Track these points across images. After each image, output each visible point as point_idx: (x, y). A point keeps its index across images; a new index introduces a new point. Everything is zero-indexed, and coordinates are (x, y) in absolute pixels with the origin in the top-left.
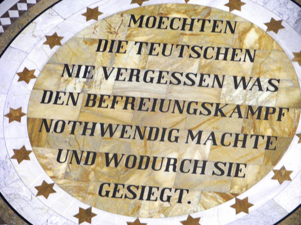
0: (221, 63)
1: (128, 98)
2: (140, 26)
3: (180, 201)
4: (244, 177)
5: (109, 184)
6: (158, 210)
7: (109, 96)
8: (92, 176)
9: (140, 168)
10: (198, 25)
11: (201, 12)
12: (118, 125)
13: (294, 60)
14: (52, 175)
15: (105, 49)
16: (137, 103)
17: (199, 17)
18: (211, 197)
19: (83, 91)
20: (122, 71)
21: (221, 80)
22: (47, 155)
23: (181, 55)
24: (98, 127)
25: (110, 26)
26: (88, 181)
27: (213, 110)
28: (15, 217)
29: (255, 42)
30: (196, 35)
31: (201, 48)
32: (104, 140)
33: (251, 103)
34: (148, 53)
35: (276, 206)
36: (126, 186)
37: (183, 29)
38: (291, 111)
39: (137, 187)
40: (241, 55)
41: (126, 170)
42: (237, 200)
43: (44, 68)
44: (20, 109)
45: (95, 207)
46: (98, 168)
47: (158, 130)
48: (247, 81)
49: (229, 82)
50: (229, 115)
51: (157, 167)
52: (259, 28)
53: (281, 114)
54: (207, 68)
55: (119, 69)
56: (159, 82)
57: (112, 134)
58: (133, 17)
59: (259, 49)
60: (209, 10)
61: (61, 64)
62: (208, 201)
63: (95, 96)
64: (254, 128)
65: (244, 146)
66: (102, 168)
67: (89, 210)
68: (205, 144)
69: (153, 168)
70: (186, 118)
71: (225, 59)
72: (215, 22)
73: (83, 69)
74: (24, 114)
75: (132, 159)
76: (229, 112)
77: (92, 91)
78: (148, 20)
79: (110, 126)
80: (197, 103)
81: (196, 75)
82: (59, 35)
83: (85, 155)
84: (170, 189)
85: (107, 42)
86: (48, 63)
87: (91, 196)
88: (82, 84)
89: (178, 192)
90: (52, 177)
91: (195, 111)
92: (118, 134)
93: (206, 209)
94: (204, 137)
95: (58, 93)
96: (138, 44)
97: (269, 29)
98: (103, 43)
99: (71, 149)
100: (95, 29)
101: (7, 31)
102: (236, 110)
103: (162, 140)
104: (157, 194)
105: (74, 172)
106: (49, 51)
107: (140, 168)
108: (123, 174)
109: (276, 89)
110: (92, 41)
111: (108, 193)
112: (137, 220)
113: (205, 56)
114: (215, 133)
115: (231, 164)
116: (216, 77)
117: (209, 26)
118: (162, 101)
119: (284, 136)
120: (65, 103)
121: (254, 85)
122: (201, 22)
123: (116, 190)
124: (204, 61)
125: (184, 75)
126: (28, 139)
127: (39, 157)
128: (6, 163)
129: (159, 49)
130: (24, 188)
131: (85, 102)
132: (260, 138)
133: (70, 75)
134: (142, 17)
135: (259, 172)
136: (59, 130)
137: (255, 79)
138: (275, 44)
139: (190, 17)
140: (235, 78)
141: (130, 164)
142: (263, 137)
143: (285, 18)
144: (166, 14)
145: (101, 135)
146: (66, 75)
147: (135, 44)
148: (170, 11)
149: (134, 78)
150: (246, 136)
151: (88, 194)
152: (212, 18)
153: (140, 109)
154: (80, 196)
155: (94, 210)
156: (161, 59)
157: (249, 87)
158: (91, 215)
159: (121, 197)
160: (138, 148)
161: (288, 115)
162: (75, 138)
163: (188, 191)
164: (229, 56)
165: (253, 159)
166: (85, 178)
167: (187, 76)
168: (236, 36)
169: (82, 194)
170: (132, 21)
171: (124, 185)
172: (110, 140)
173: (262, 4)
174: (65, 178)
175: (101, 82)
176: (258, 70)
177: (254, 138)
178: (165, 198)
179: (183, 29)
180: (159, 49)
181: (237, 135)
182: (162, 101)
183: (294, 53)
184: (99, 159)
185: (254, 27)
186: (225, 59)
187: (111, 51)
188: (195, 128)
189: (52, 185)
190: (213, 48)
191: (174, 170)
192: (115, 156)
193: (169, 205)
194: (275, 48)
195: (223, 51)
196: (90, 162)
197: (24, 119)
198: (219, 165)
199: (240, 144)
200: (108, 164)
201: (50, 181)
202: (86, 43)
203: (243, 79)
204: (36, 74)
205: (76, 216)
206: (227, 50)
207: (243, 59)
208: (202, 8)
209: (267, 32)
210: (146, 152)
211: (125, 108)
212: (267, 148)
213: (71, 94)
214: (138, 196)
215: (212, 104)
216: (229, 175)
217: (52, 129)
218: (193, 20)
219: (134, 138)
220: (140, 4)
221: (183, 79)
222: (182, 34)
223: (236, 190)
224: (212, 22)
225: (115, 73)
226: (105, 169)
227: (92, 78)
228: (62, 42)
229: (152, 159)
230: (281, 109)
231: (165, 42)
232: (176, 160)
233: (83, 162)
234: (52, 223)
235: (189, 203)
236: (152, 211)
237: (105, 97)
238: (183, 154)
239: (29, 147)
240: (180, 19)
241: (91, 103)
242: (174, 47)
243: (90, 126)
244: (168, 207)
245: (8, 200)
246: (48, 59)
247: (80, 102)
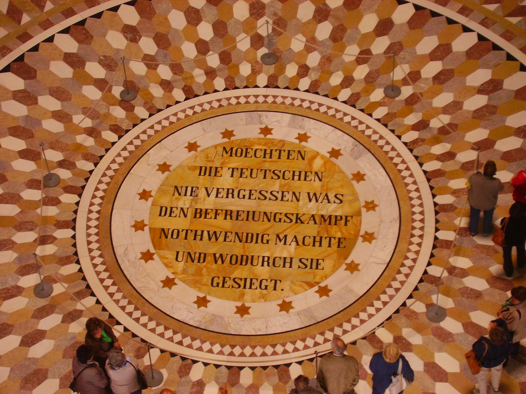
0: (296, 183)
1: (226, 211)
2: (231, 155)
3: (275, 289)
4: (323, 269)
5: (219, 277)
6: (258, 296)
7: (212, 210)
8: (204, 271)
9: (241, 264)
10: (275, 154)
11: (277, 144)
12: (221, 232)
13: (353, 179)
14: (173, 272)
15: (205, 174)
16: (234, 215)
17: (276, 148)
19: (191, 206)
20: (220, 190)
21: (298, 195)
22: (167, 256)
23: (265, 178)
24: (206, 234)
25: (207, 155)
26: (202, 275)
27: (294, 218)
28: (147, 304)
29: (321, 167)
30: (275, 162)
31: (280, 171)
33: (323, 213)
34: (239, 176)
35: (350, 291)
36: (232, 279)
37: (264, 157)
38: (354, 218)
39: (241, 279)
40: (311, 177)
41: (231, 266)
42: (319, 287)
43: (159, 189)
44: (143, 221)
45: (209, 295)
46: (209, 265)
47: (252, 235)
48: (318, 196)
49: (304, 197)
50: (307, 222)
51: (255, 263)
52: (323, 155)
53: (346, 221)
54: (286, 187)
55: (218, 189)
56: (250, 198)
57: (217, 239)
58: (224, 148)
59: (325, 171)
60: (283, 142)
61: (171, 186)
62: (297, 288)
63: (201, 210)
64: (327, 232)
65: (320, 246)
66: (212, 265)
67: (204, 298)
68: (290, 245)
69: (252, 264)
70: (273, 225)
71: (299, 179)
72: (289, 151)
73: (189, 189)
74: (146, 225)
75: (234, 258)
76: (306, 220)
77: (199, 206)
78: (237, 150)
79: (215, 233)
80: (281, 213)
81: (278, 192)
82: (168, 164)
83: (197, 255)
84: (267, 280)
85: (206, 168)
86: (161, 186)
87: (205, 287)
88: (190, 201)
89: (273, 281)
90: (173, 273)
91: (280, 219)
92: (221, 239)
93: (296, 294)
94: (289, 240)
95: (171, 208)
96: (231, 170)
97: (331, 157)
98: (203, 169)
99: (186, 251)
100: (196, 158)
101: (127, 161)
102: (312, 219)
103: (257, 242)
104: (257, 284)
106: (162, 176)
107: (241, 264)
108: (229, 269)
109: (341, 202)
111: (218, 284)
112: (243, 305)
113: (284, 178)
114: (297, 236)
115: (312, 260)
116: (294, 193)
117: (284, 155)
118: (254, 212)
119: (351, 237)
120: (178, 216)
121: (324, 199)
122: (278, 151)
123: (224, 282)
124: (283, 181)
125: (269, 192)
126: (151, 244)
127: (161, 257)
128: (136, 263)
129: (247, 173)
130: (152, 282)
131: (194, 215)
132: (332, 239)
133: (180, 194)
134: (232, 149)
136: (175, 236)
137: (324, 194)
138: (336, 168)
139: (269, 148)
140: (309, 193)
141: (234, 261)
142: (335, 238)
143: (342, 147)
144: (250, 146)
145: (208, 240)
146: (176, 194)
147: (228, 169)
148: (253, 144)
149: (230, 195)
150: (321, 238)
152: (287, 148)
153: (237, 219)
155: (208, 298)
156: (249, 180)
157: (320, 200)
160: (239, 249)
161: (352, 221)
162: (189, 242)
163: (280, 281)
164: (303, 177)
165: (329, 255)
166: (199, 273)
167: (271, 193)
168: (306, 162)
170: (224, 152)
171: (230, 278)
173: (324, 137)
174: (183, 274)
175: (204, 199)
176: (325, 188)
177: (328, 239)
178: (263, 287)
179: (264, 157)
180: (247, 173)
181: (315, 237)
182: (254, 212)
183: (352, 174)
184: (209, 258)
185: (319, 155)
186: (299, 179)
187: (210, 175)
189: (174, 279)
190: (289, 171)
191: (268, 265)
192: (221, 255)
193: (267, 293)
194: (337, 170)
195: (297, 174)
196: (201, 261)
197: (147, 229)
198: (303, 260)
199: (317, 244)
200: (216, 262)
201: (172, 276)
202: (190, 170)
203: (315, 194)
204: (153, 194)
205: (195, 302)
206: (300, 172)
207: (313, 180)
208: (277, 141)
209: (330, 159)
210: (245, 251)
211: (225, 219)
212: (339, 246)
213: (182, 209)
214: (242, 286)
215: (293, 214)
216: (311, 268)
217: (169, 236)
218: (272, 150)
219: (234, 242)
220: (229, 139)
221: (268, 195)
222: (264, 161)
223: (317, 279)
224: (287, 152)
225: (214, 192)
226: (214, 266)
227: (197, 196)
228: (171, 169)
229: (250, 258)
230: (346, 217)
231: (252, 168)
232: (269, 258)
233: (196, 261)
234: (176, 308)
235: (282, 290)
237: (209, 211)
238: (273, 253)
239: (152, 250)
240: (261, 150)
241: (198, 215)
242: (259, 171)
243: (199, 233)
244: (266, 294)
245: (140, 291)
246: (161, 183)
247: (190, 214)
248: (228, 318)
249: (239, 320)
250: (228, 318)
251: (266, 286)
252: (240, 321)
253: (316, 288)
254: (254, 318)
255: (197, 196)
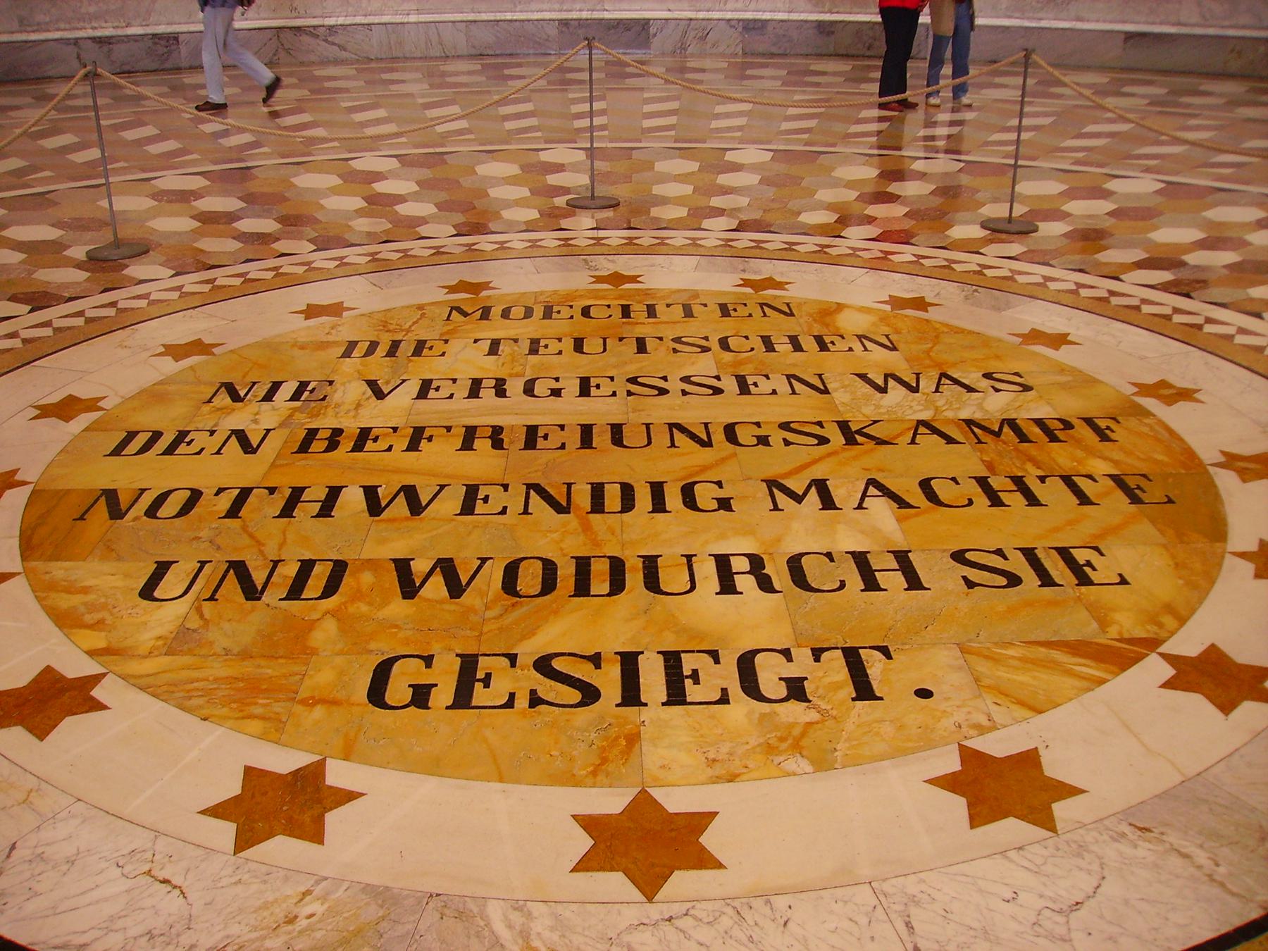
3: (864, 690)
5: (428, 660)
6: (753, 742)
8: (326, 634)
18: (1023, 660)
19: (282, 425)
32: (383, 525)
39: (596, 660)
51: (674, 578)
66: (385, 603)
67: (309, 779)
77: (327, 422)
84: (786, 653)
87: (319, 712)
93: (1041, 712)
105: (227, 626)
107: (582, 588)
110: (323, 346)
111: (421, 696)
124: (727, 357)
135: (1177, 565)
151: (304, 702)
154: (251, 717)
155: (338, 774)
158: (319, 801)
159: (510, 704)
162: (244, 528)
163: (885, 651)
169: (264, 705)
171: (513, 659)
172: (416, 522)
188: (789, 474)
193: (813, 716)
219: (526, 512)
226: (399, 608)
235: (924, 694)
236: (725, 749)
244: (810, 724)
248: (518, 906)
249: (631, 914)
250: (518, 906)
251: (796, 690)
252: (632, 928)
253: (1155, 669)
254: (767, 896)
255: (324, 399)
